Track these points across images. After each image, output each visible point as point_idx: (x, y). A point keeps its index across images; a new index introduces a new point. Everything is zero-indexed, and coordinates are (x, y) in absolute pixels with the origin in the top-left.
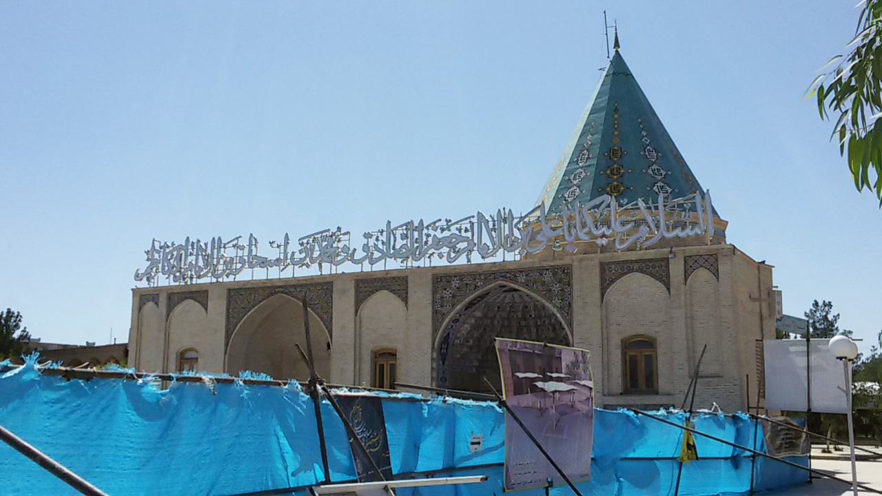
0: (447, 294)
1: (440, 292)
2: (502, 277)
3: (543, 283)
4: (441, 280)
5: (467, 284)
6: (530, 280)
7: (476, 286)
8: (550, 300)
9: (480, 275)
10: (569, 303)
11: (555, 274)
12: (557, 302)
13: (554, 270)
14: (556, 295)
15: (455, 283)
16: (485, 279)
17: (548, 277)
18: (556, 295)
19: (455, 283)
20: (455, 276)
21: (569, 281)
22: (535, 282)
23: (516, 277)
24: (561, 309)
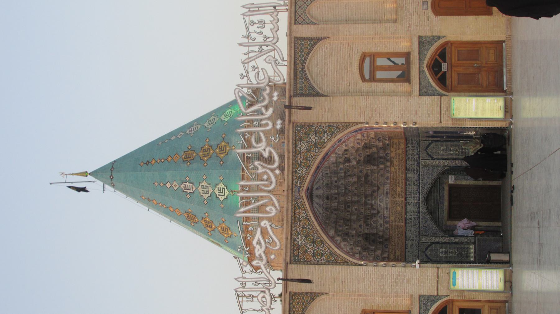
0: (311, 249)
1: (308, 257)
2: (299, 191)
3: (308, 150)
4: (297, 256)
5: (303, 228)
6: (304, 163)
7: (306, 218)
8: (324, 144)
9: (295, 214)
10: (328, 126)
11: (301, 139)
12: (326, 137)
13: (297, 139)
14: (320, 138)
15: (301, 240)
16: (299, 208)
17: (303, 146)
18: (320, 138)
19: (301, 240)
20: (295, 240)
21: (309, 126)
22: (306, 159)
23: (300, 177)
24: (333, 134)
